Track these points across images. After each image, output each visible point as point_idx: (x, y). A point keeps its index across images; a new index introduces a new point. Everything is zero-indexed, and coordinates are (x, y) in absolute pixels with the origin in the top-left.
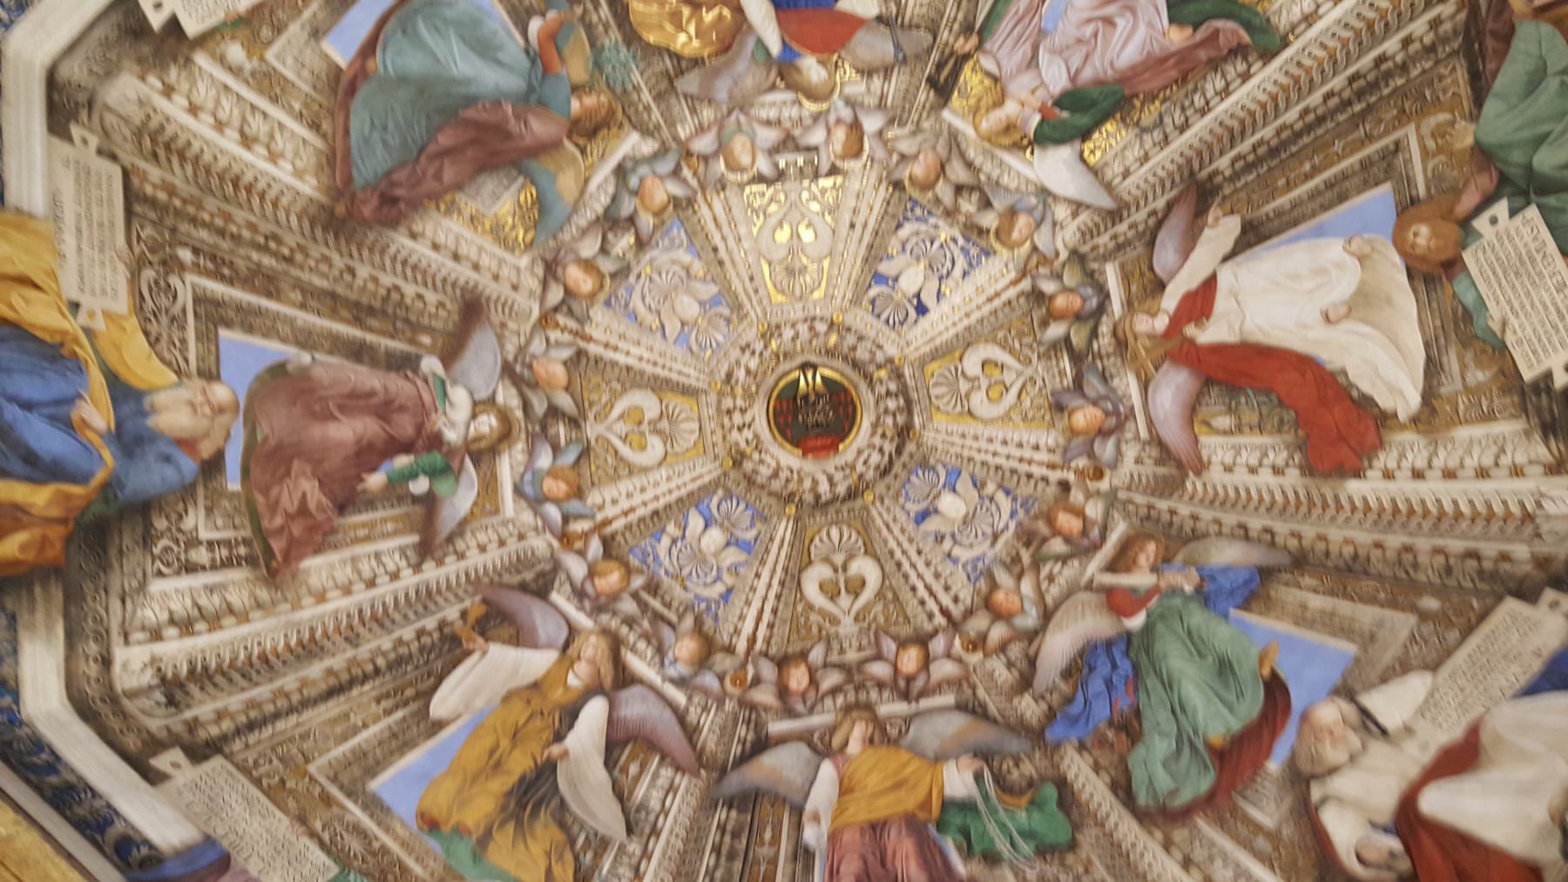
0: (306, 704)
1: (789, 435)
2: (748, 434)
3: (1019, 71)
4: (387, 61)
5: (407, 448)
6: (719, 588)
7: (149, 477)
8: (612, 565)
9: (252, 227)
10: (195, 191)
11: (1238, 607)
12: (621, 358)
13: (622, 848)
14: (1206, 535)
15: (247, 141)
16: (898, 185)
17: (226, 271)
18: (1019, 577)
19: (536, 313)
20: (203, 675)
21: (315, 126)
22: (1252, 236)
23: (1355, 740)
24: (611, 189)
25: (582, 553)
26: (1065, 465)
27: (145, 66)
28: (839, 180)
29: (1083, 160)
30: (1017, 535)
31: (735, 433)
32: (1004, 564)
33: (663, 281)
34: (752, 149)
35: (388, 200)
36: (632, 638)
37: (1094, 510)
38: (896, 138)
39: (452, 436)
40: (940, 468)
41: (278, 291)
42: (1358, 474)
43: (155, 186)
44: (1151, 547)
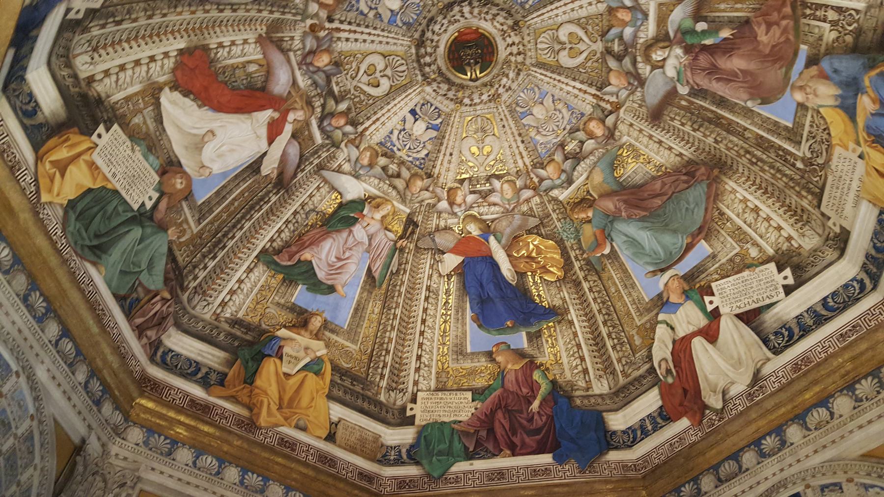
1: (486, 41)
2: (509, 41)
4: (682, 241)
5: (705, 48)
9: (763, 170)
10: (787, 191)
15: (756, 210)
16: (429, 176)
17: (781, 153)
19: (622, 110)
21: (722, 214)
22: (255, 167)
24: (575, 173)
27: (798, 252)
28: (458, 178)
29: (340, 194)
31: (517, 42)
33: (552, 126)
34: (503, 191)
35: (691, 174)
37: (314, 8)
39: (678, 51)
40: (400, 25)
41: (756, 139)
43: (806, 198)
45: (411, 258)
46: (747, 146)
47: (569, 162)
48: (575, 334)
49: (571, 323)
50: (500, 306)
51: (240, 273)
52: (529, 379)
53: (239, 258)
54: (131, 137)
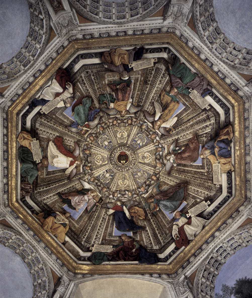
0: (192, 118)
2: (133, 156)
6: (139, 135)
7: (210, 144)
8: (153, 139)
12: (149, 168)
16: (108, 188)
17: (201, 173)
18: (99, 132)
19: (160, 173)
21: (189, 194)
22: (64, 170)
23: (67, 101)
25: (157, 140)
29: (83, 186)
37: (88, 139)
39: (173, 156)
45: (99, 209)
46: (192, 175)
47: (147, 187)
48: (148, 234)
49: (147, 231)
50: (125, 225)
52: (132, 244)
53: (52, 192)
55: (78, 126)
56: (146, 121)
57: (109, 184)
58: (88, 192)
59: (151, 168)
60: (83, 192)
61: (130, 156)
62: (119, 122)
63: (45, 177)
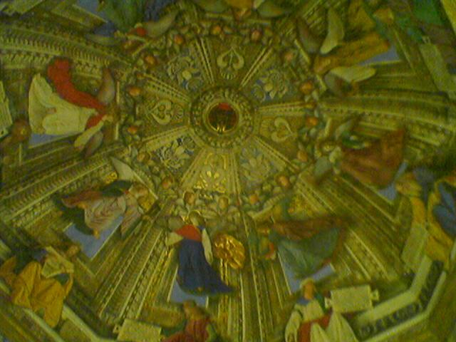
0: (411, 91)
2: (246, 117)
3: (132, 206)
7: (427, 175)
11: (105, 23)
13: (332, 6)
14: (108, 47)
16: (177, 181)
18: (172, 46)
19: (300, 175)
20: (436, 113)
21: (345, 249)
22: (71, 139)
25: (312, 98)
26: (146, 79)
28: (195, 187)
29: (118, 174)
30: (168, 61)
32: (175, 53)
36: (305, 67)
37: (141, 62)
38: (173, 195)
39: (338, 149)
40: (187, 88)
42: (55, 57)
44: (126, 47)
45: (149, 228)
49: (240, 300)
51: (36, 202)
54: (7, 92)
55: (116, 31)
56: (299, 46)
57: (181, 171)
58: (128, 189)
59: (281, 156)
60: (117, 189)
61: (241, 116)
62: (227, 30)
63: (20, 164)
